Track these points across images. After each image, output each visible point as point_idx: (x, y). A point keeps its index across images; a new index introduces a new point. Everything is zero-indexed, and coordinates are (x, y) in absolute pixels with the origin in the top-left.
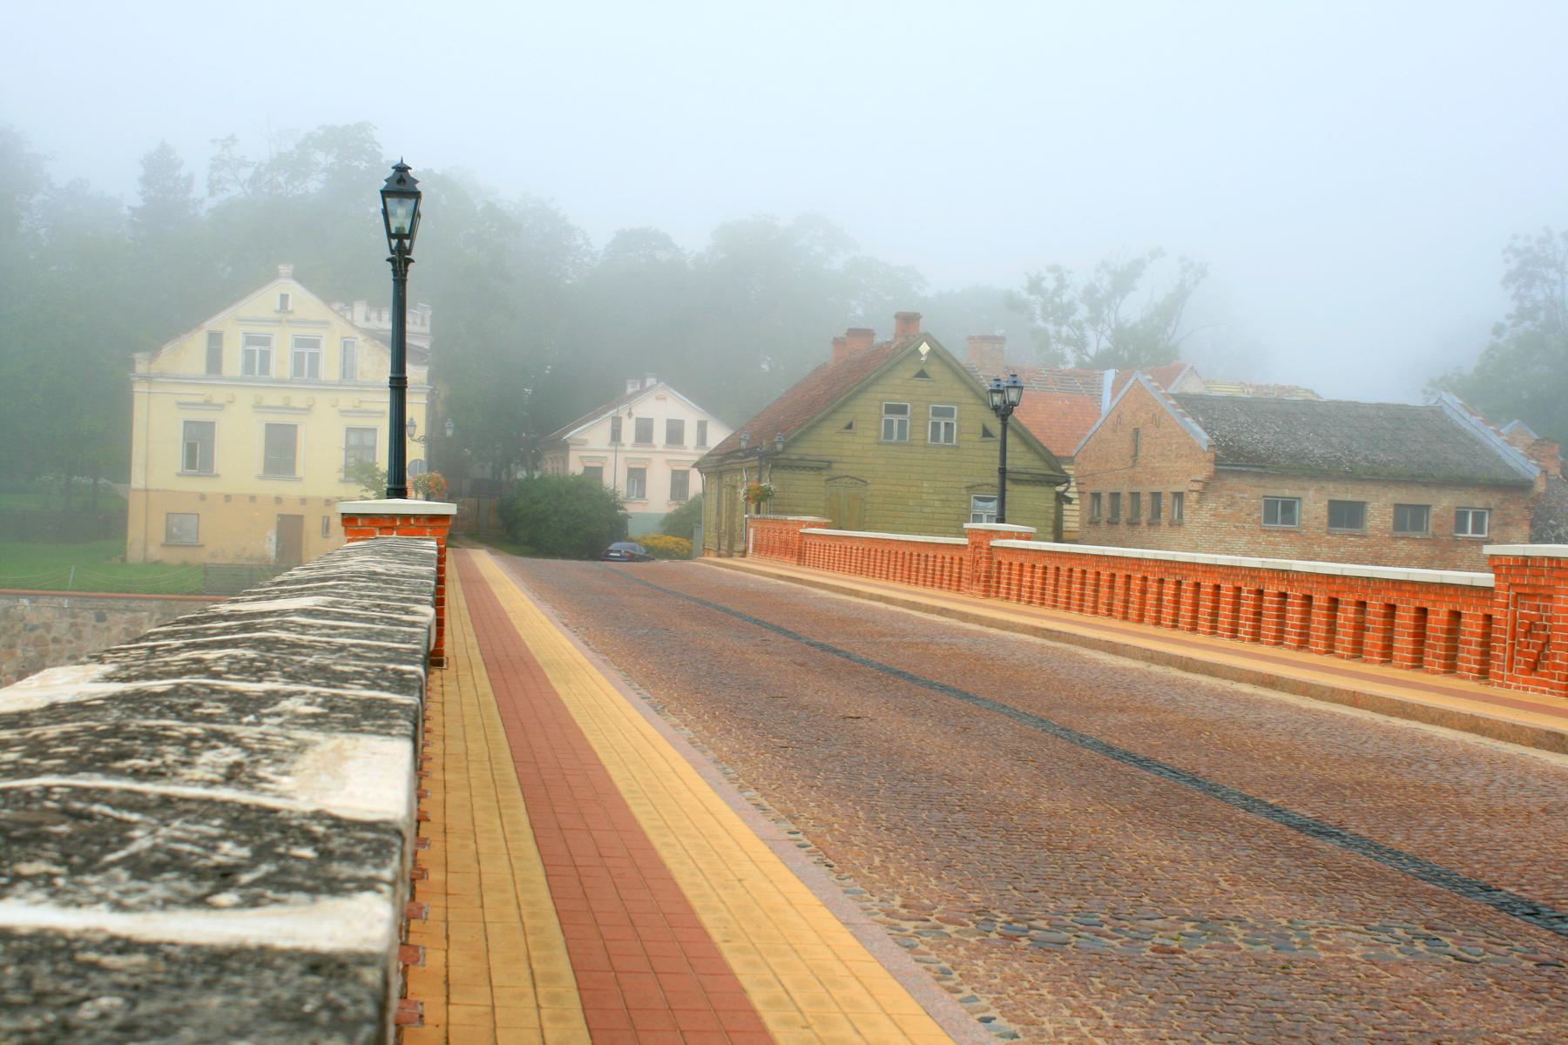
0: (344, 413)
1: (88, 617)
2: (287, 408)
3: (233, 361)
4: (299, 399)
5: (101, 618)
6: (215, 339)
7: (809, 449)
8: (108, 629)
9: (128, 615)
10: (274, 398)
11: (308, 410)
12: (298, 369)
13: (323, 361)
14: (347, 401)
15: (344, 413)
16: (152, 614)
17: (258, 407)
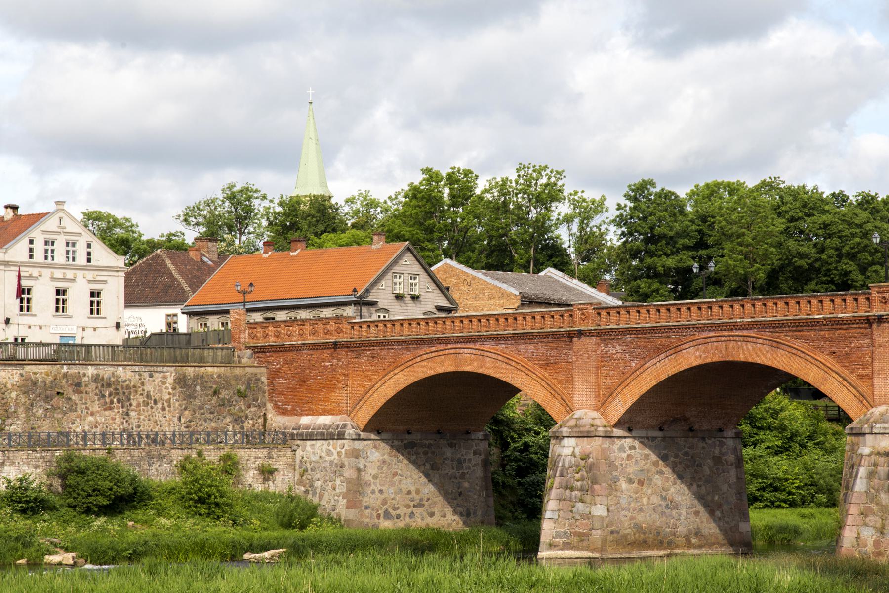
0: (90, 281)
1: (146, 375)
2: (64, 279)
3: (39, 256)
4: (70, 274)
5: (151, 376)
6: (31, 242)
7: (371, 298)
8: (154, 381)
9: (162, 374)
10: (58, 274)
11: (73, 280)
12: (46, 258)
13: (77, 256)
14: (90, 275)
15: (90, 281)
16: (172, 373)
17: (53, 279)
